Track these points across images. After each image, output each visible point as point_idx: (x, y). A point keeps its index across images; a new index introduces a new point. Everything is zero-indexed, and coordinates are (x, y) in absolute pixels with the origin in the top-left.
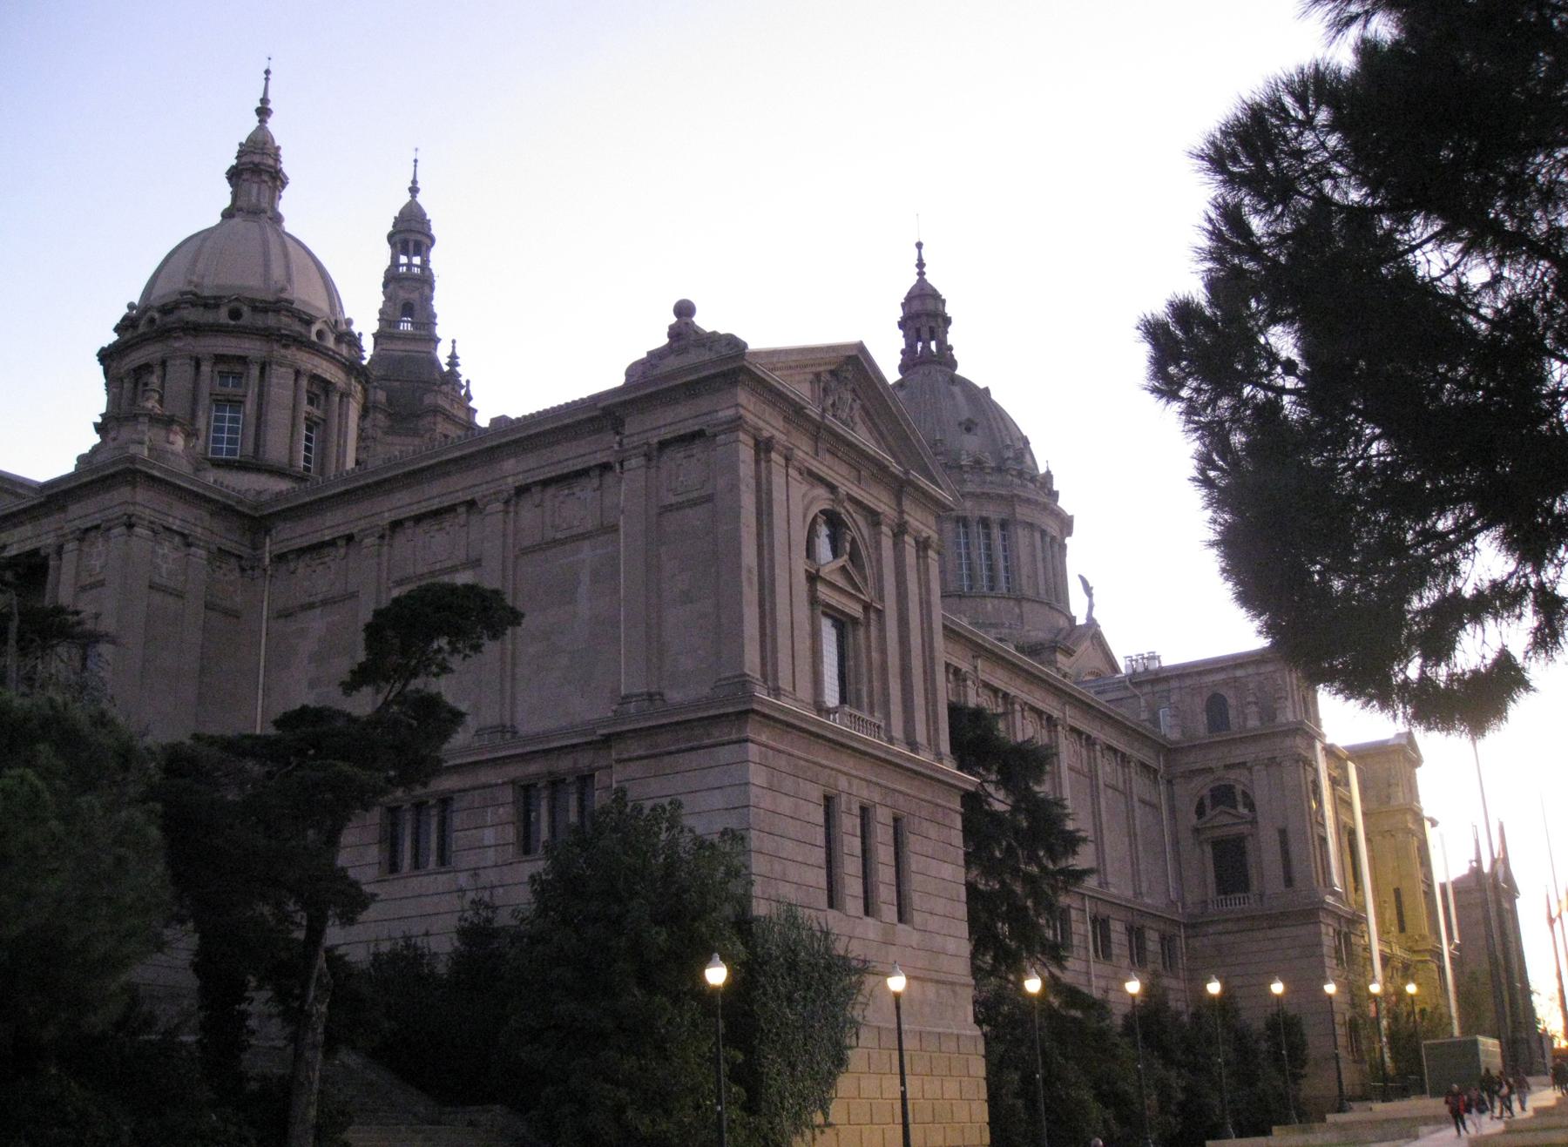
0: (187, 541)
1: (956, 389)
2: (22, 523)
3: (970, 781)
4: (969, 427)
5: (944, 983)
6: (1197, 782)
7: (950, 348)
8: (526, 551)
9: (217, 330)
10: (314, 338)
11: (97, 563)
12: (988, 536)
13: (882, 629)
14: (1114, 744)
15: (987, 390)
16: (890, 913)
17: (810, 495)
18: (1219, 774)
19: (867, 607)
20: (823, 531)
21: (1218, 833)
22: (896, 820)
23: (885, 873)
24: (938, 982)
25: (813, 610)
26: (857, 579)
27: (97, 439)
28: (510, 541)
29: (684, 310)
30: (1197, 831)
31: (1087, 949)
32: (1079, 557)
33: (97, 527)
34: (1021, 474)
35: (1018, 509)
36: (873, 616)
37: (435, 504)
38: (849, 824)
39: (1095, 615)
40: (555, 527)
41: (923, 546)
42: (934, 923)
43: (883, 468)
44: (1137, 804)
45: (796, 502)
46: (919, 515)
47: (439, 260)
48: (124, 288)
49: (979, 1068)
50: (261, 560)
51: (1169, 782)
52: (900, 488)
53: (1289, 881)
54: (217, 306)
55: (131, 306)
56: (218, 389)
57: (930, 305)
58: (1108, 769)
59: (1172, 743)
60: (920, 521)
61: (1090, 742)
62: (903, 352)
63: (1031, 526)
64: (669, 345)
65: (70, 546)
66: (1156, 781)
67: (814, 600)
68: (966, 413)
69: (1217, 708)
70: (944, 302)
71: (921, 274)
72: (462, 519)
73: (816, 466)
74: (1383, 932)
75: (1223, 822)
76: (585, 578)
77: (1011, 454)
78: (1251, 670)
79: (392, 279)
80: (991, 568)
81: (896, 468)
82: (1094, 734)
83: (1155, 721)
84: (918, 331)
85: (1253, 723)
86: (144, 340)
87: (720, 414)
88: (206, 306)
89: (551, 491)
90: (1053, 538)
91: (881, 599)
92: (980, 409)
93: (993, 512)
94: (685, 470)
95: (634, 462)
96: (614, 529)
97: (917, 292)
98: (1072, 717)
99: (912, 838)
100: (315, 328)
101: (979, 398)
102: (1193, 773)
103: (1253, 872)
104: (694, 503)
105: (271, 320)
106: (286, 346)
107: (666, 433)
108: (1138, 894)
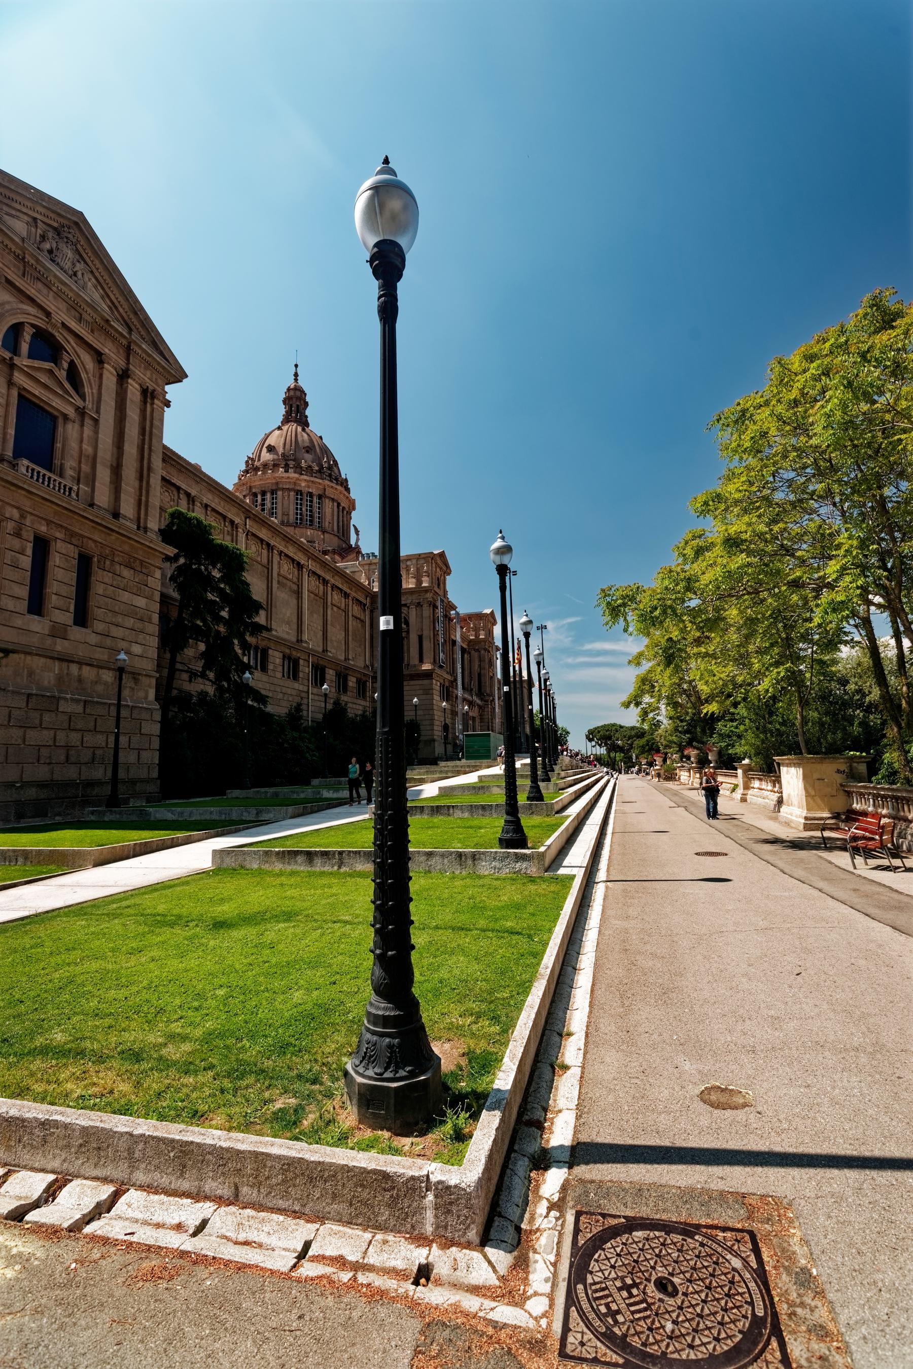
7: (306, 417)
12: (311, 501)
13: (96, 432)
14: (340, 586)
19: (81, 412)
34: (330, 475)
36: (88, 421)
39: (359, 543)
57: (298, 393)
58: (336, 597)
61: (325, 582)
63: (333, 500)
67: (10, 383)
71: (296, 380)
74: (463, 688)
82: (327, 578)
90: (344, 508)
98: (312, 565)
108: (347, 659)
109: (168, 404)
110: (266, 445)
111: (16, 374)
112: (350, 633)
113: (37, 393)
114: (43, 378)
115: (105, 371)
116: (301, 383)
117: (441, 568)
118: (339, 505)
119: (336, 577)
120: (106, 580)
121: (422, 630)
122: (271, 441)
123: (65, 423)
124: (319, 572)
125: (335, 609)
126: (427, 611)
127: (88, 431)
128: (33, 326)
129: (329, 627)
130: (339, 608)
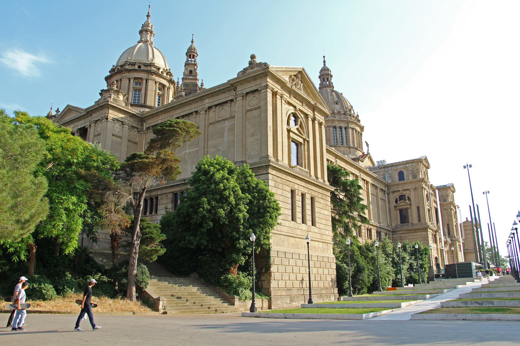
0: (123, 123)
1: (334, 93)
2: (81, 120)
3: (333, 189)
7: (332, 83)
8: (211, 124)
9: (135, 70)
10: (160, 73)
11: (99, 129)
12: (341, 131)
13: (308, 146)
16: (309, 223)
17: (288, 109)
18: (401, 192)
19: (304, 140)
20: (292, 118)
21: (401, 207)
23: (308, 212)
27: (100, 97)
28: (207, 121)
29: (253, 57)
30: (395, 207)
33: (99, 120)
34: (350, 115)
37: (187, 112)
38: (298, 198)
39: (369, 152)
41: (320, 124)
42: (322, 226)
43: (309, 102)
44: (379, 199)
45: (285, 110)
46: (319, 116)
47: (198, 59)
48: (113, 62)
49: (334, 266)
50: (143, 129)
51: (388, 194)
52: (314, 108)
53: (419, 221)
54: (135, 65)
55: (113, 66)
56: (135, 86)
57: (327, 72)
60: (320, 118)
62: (320, 84)
63: (353, 129)
64: (249, 66)
65: (92, 125)
67: (289, 137)
68: (336, 99)
69: (401, 176)
71: (325, 64)
72: (194, 116)
73: (290, 101)
75: (402, 205)
76: (226, 131)
78: (410, 165)
79: (186, 64)
80: (342, 139)
81: (313, 103)
83: (385, 179)
86: (116, 73)
87: (263, 84)
88: (132, 65)
89: (217, 108)
90: (359, 132)
91: (309, 138)
93: (343, 125)
94: (253, 100)
95: (239, 99)
96: (234, 117)
99: (316, 203)
100: (161, 71)
101: (339, 95)
102: (394, 192)
103: (410, 218)
104: (255, 109)
105: (149, 68)
106: (152, 75)
107: (248, 90)
111: (291, 133)
116: (327, 65)
117: (425, 166)
124: (364, 178)
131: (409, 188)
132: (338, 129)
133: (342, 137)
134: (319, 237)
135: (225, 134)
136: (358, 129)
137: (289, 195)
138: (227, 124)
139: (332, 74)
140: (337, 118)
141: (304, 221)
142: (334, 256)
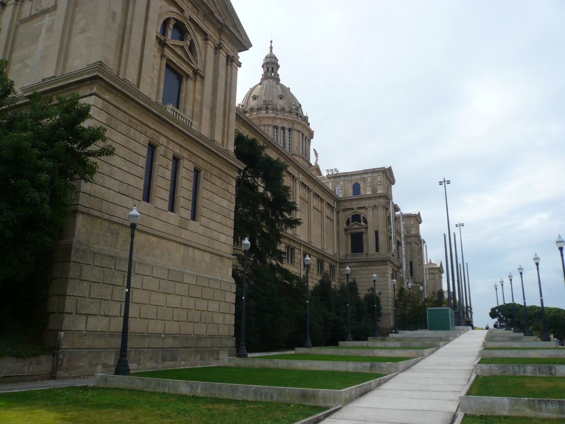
1: (278, 86)
4: (281, 98)
5: (216, 254)
6: (348, 213)
7: (278, 75)
12: (284, 133)
13: (203, 86)
14: (318, 194)
15: (289, 88)
16: (187, 214)
18: (355, 210)
21: (354, 231)
22: (197, 171)
24: (212, 253)
25: (161, 59)
26: (190, 55)
28: (16, 17)
31: (301, 264)
32: (314, 144)
34: (297, 114)
35: (295, 125)
36: (198, 78)
40: (36, 9)
42: (213, 225)
44: (325, 218)
49: (232, 298)
51: (338, 212)
53: (377, 250)
57: (273, 60)
58: (315, 202)
59: (340, 198)
61: (309, 190)
63: (299, 131)
66: (333, 211)
68: (280, 93)
69: (356, 188)
70: (278, 60)
71: (271, 51)
75: (356, 227)
77: (294, 107)
78: (370, 175)
82: (311, 188)
84: (268, 68)
85: (369, 193)
92: (285, 94)
93: (287, 125)
97: (269, 56)
98: (301, 178)
101: (286, 90)
102: (346, 210)
109: (239, 65)
110: (253, 95)
112: (325, 229)
113: (175, 61)
114: (179, 51)
115: (209, 46)
118: (303, 135)
119: (316, 187)
120: (208, 188)
121: (378, 226)
122: (255, 93)
123: (187, 80)
125: (315, 210)
126: (381, 212)
127: (198, 85)
128: (174, 18)
129: (312, 224)
130: (317, 210)
131: (366, 205)
132: (279, 130)
133: (284, 140)
134: (206, 244)
135: (41, 38)
136: (306, 134)
137: (144, 151)
138: (47, 19)
139: (279, 63)
140: (279, 116)
141: (172, 208)
142: (233, 281)
